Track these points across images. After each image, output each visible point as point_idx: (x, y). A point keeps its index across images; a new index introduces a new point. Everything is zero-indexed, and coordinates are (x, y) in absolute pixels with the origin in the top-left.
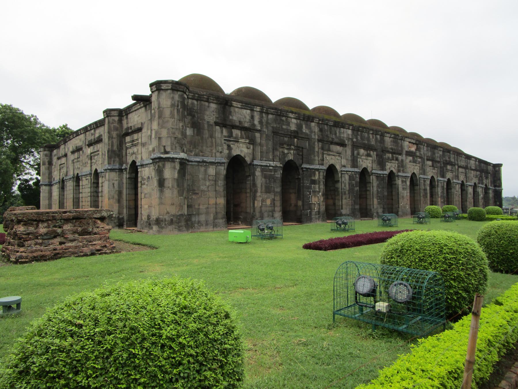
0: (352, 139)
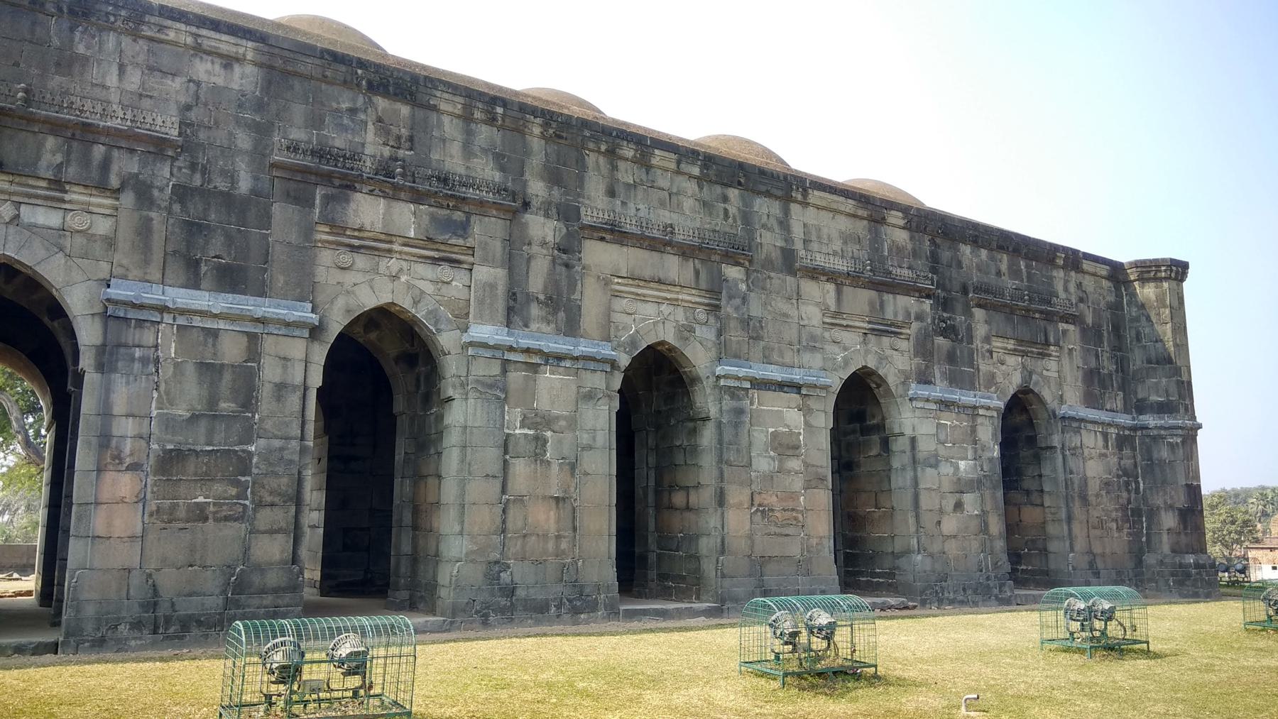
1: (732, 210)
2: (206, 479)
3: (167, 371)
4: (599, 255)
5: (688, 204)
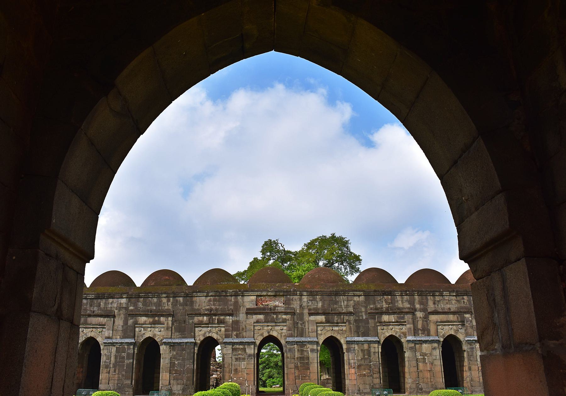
0: (126, 308)
1: (465, 301)
2: (365, 369)
3: (356, 352)
4: (433, 318)
5: (453, 302)
